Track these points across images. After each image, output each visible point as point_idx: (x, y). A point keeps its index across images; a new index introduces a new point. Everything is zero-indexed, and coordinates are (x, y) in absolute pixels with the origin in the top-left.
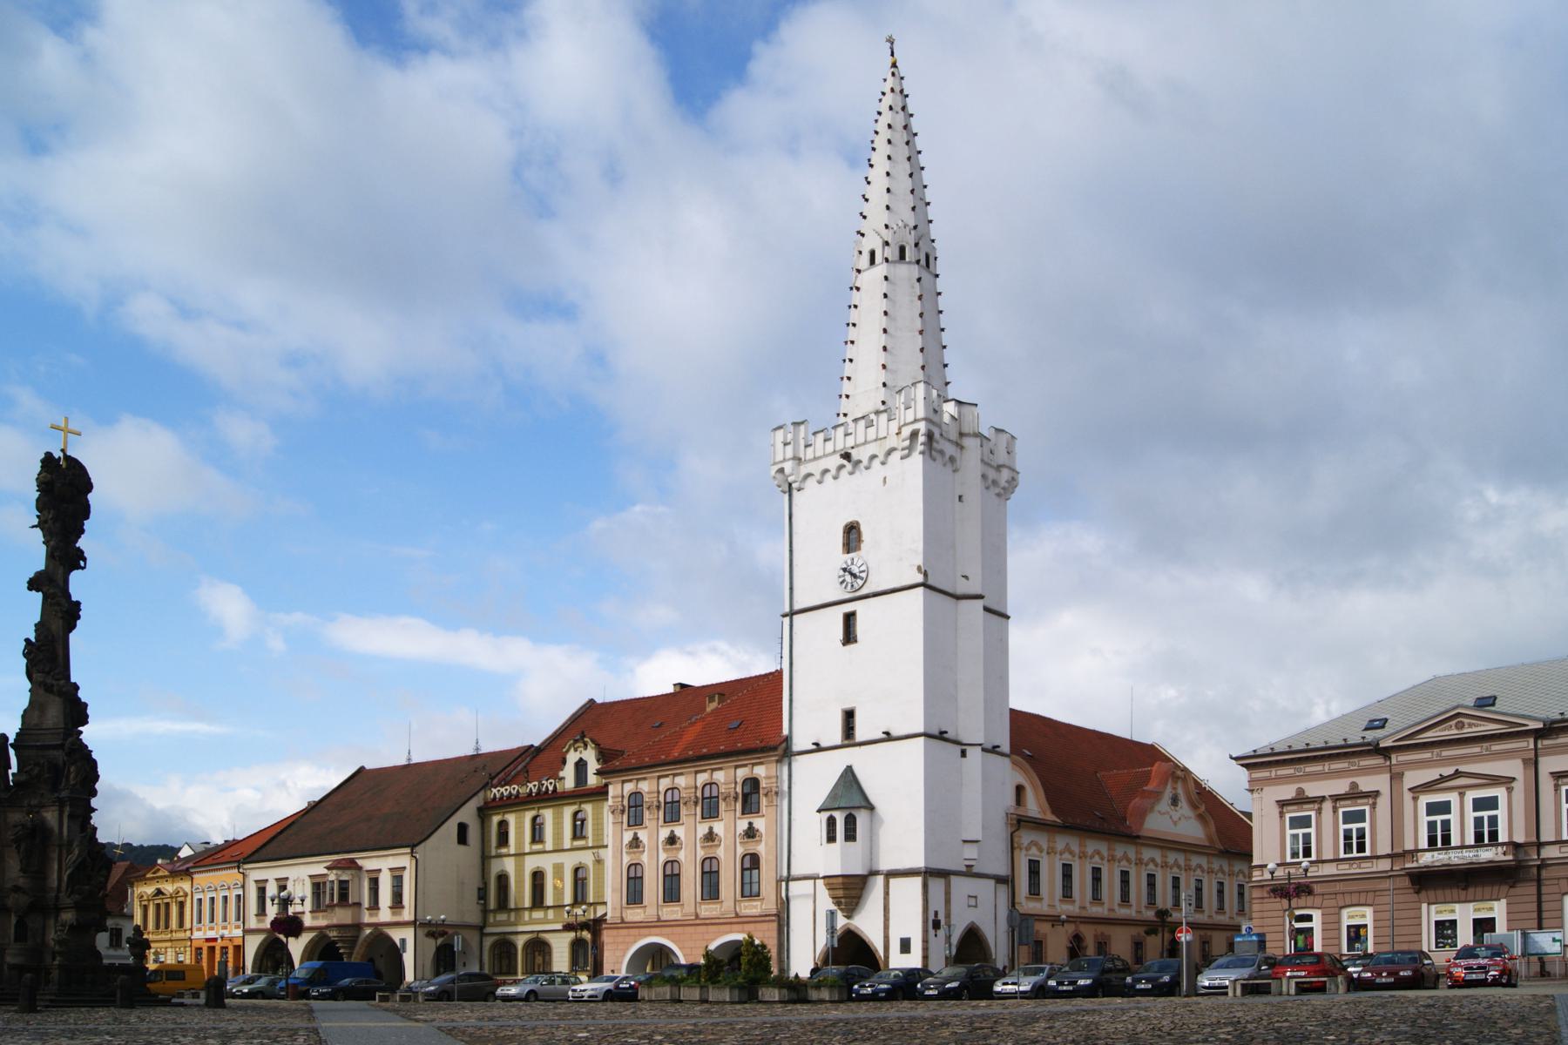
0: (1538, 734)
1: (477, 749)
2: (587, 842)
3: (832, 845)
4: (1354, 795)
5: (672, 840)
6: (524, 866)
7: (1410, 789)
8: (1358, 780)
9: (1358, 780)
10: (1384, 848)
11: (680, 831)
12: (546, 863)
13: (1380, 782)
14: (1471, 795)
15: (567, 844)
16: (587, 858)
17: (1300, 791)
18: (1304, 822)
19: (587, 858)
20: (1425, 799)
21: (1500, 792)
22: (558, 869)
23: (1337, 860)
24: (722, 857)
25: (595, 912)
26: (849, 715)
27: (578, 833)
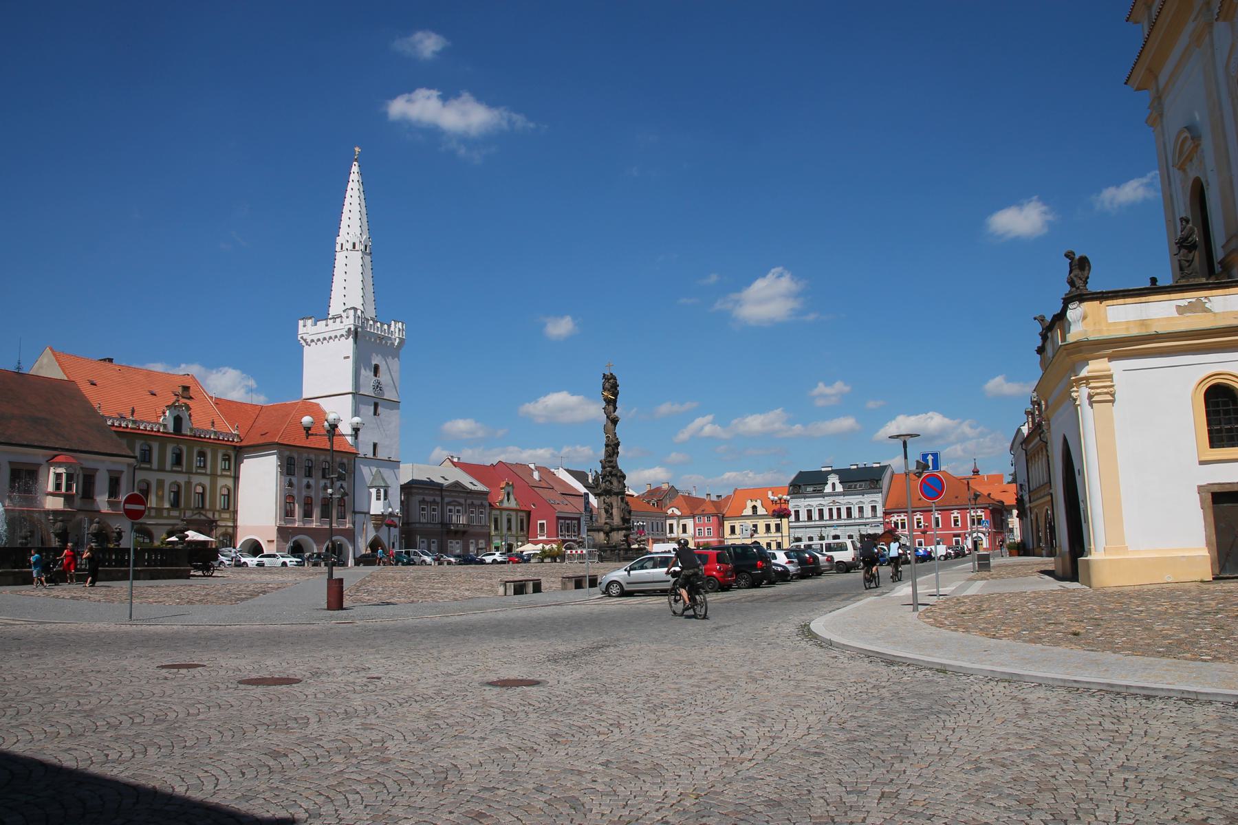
0: (468, 493)
1: (19, 368)
2: (182, 469)
3: (378, 501)
4: (434, 502)
5: (308, 486)
6: (217, 483)
7: (446, 503)
8: (425, 497)
9: (425, 497)
10: (440, 521)
11: (312, 482)
12: (153, 477)
13: (438, 499)
14: (457, 508)
15: (168, 467)
16: (181, 479)
17: (424, 498)
18: (423, 509)
19: (181, 479)
20: (449, 507)
21: (460, 508)
22: (161, 484)
23: (431, 523)
24: (313, 497)
25: (185, 514)
26: (375, 445)
27: (178, 460)
